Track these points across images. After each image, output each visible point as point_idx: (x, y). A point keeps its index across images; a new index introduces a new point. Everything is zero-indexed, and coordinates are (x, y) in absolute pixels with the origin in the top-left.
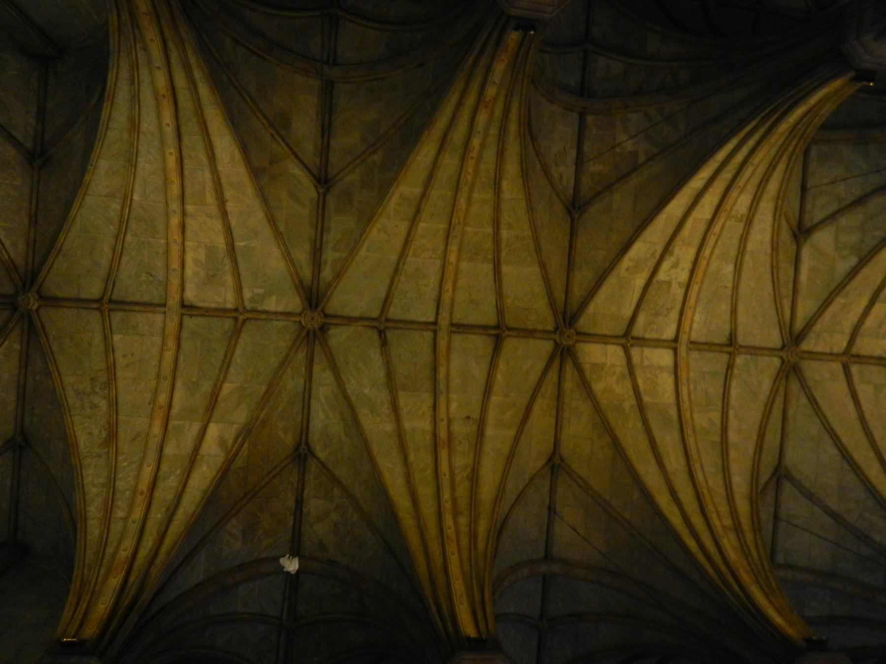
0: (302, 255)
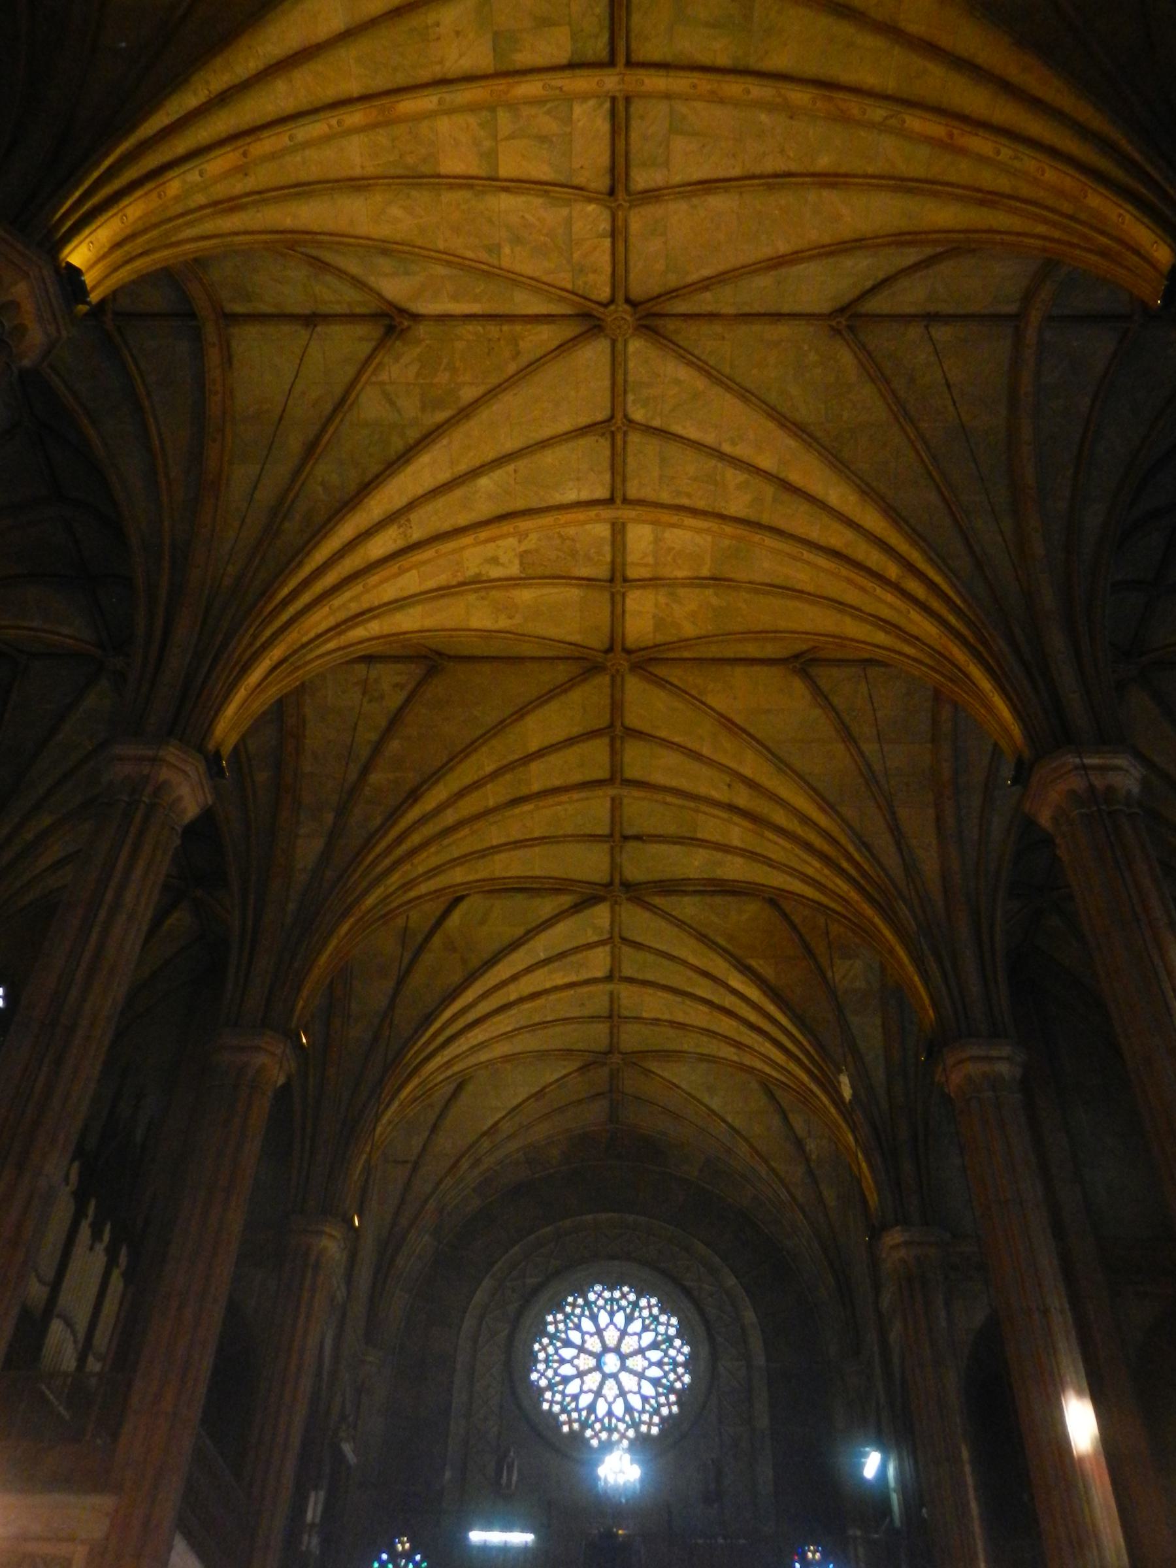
0: (547, 906)
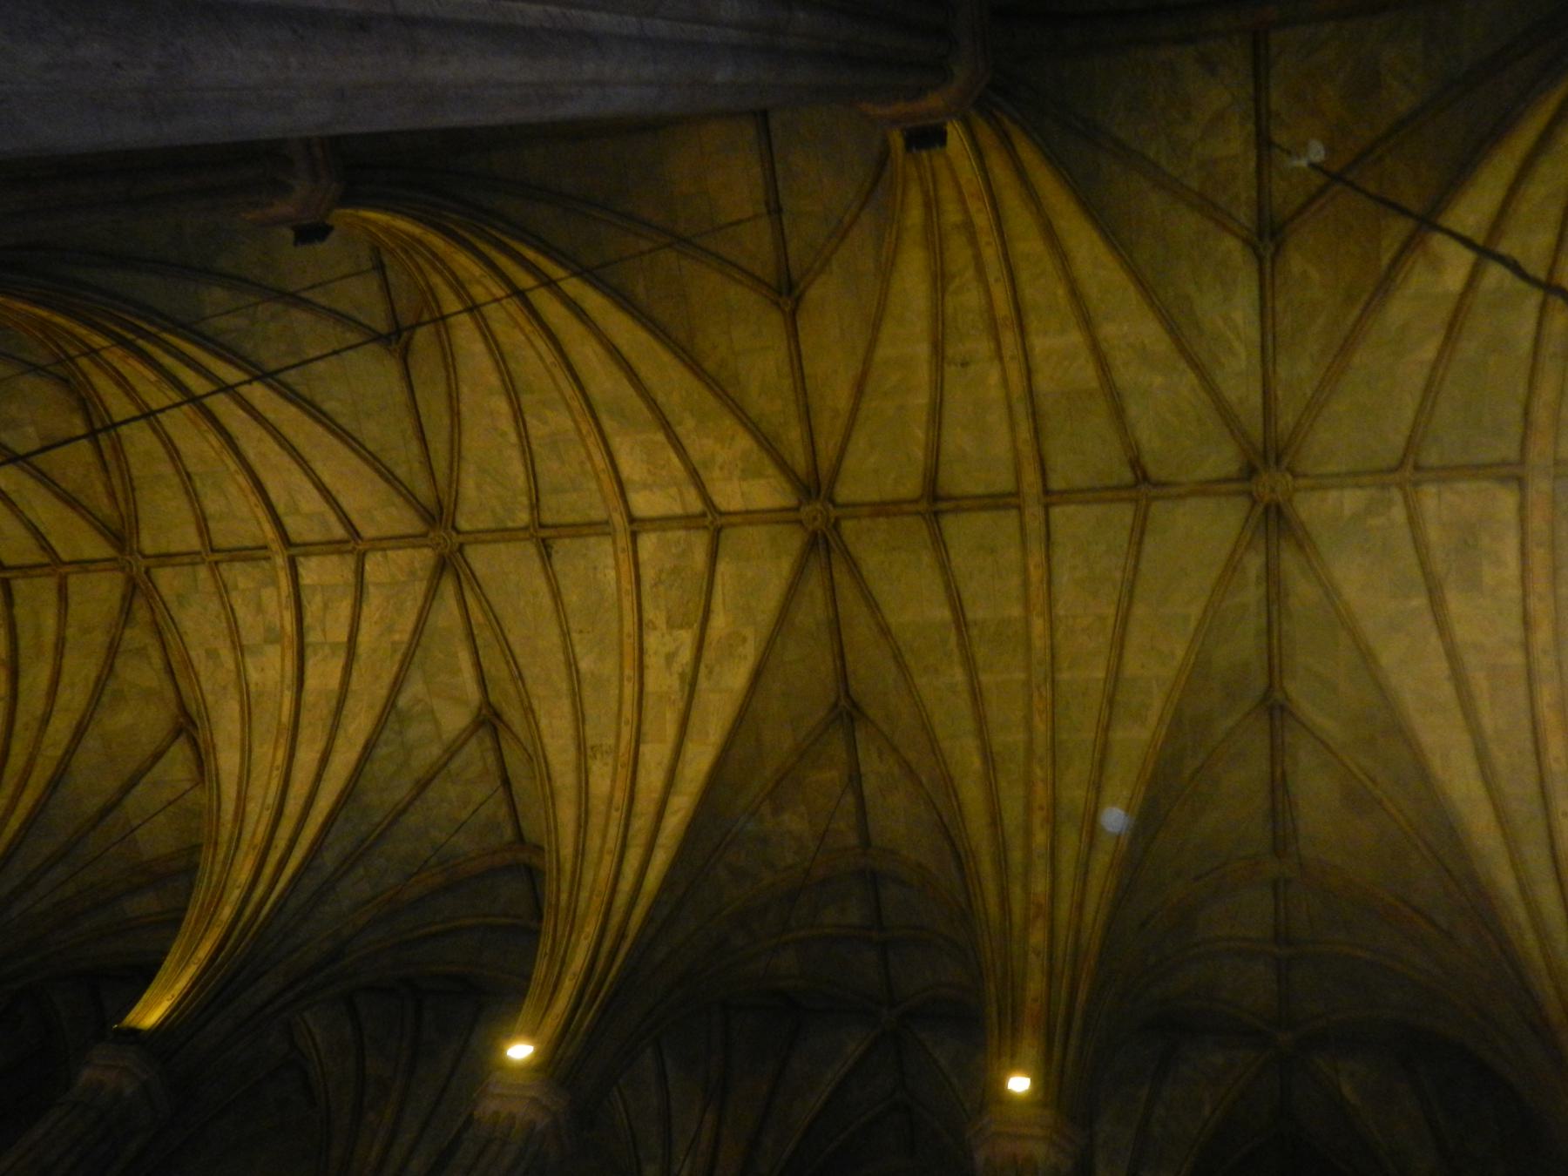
0: (1302, 590)
